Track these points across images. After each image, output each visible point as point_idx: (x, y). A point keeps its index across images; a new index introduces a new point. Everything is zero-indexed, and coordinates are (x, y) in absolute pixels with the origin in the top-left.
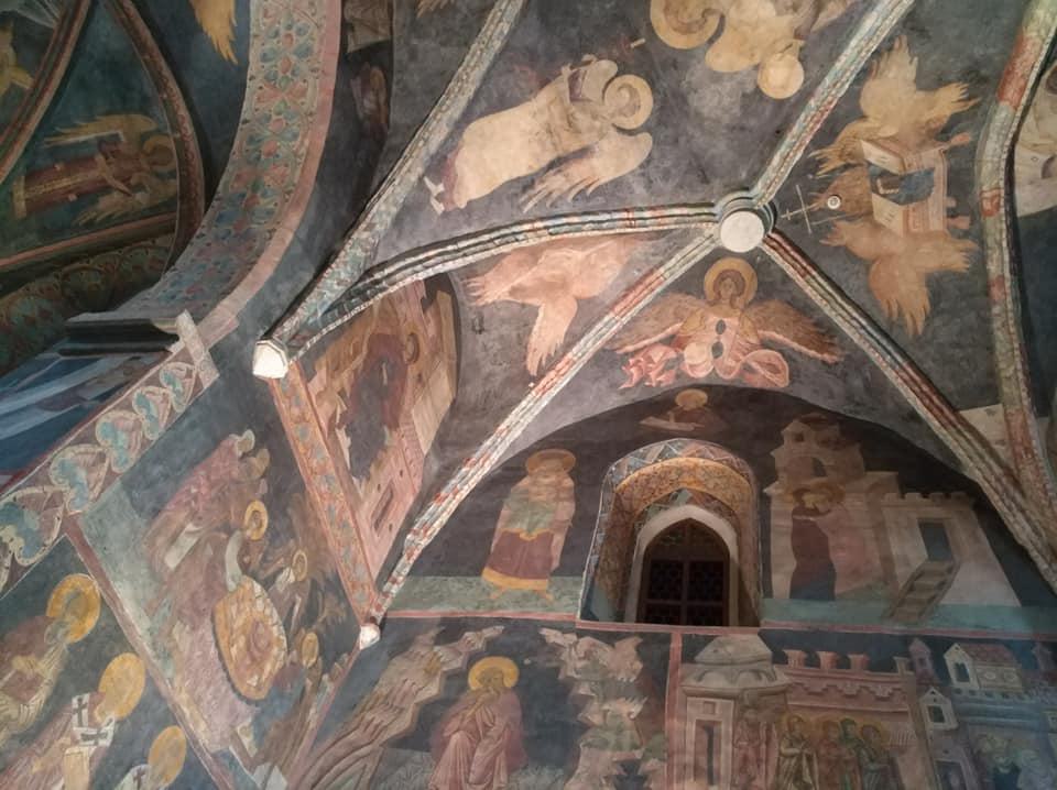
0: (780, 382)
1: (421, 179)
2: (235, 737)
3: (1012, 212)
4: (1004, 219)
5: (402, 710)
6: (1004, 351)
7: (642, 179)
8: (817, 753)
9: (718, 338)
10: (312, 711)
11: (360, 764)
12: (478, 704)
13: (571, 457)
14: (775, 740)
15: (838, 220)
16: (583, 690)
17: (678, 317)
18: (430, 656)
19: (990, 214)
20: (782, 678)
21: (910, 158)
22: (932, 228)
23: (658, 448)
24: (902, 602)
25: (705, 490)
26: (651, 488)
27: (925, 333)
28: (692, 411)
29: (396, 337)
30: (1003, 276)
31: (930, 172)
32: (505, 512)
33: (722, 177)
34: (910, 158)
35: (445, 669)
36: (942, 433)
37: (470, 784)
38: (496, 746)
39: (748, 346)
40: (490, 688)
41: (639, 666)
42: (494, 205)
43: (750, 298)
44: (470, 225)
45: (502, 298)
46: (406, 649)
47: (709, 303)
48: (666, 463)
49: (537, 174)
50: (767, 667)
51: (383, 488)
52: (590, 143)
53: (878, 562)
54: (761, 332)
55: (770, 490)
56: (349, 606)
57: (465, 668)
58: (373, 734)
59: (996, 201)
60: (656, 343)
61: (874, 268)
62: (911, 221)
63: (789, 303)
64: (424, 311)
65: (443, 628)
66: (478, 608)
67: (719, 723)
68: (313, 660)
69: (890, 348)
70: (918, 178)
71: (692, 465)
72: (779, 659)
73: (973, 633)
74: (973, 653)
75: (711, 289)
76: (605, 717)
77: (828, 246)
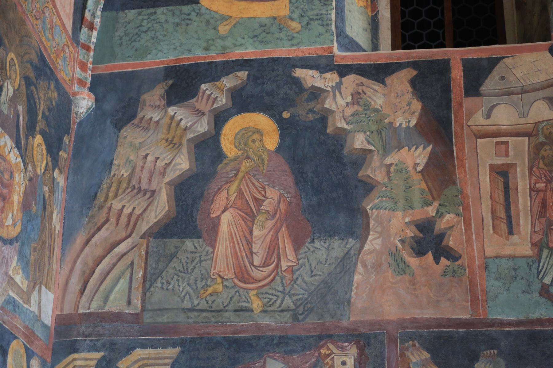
2: (11, 281)
5: (153, 192)
10: (54, 216)
11: (126, 261)
12: (241, 175)
18: (166, 121)
35: (190, 136)
37: (256, 267)
38: (273, 221)
40: (251, 153)
41: (417, 106)
46: (134, 116)
57: (213, 132)
58: (128, 224)
65: (171, 82)
66: (207, 49)
67: (512, 166)
68: (44, 164)
76: (388, 172)
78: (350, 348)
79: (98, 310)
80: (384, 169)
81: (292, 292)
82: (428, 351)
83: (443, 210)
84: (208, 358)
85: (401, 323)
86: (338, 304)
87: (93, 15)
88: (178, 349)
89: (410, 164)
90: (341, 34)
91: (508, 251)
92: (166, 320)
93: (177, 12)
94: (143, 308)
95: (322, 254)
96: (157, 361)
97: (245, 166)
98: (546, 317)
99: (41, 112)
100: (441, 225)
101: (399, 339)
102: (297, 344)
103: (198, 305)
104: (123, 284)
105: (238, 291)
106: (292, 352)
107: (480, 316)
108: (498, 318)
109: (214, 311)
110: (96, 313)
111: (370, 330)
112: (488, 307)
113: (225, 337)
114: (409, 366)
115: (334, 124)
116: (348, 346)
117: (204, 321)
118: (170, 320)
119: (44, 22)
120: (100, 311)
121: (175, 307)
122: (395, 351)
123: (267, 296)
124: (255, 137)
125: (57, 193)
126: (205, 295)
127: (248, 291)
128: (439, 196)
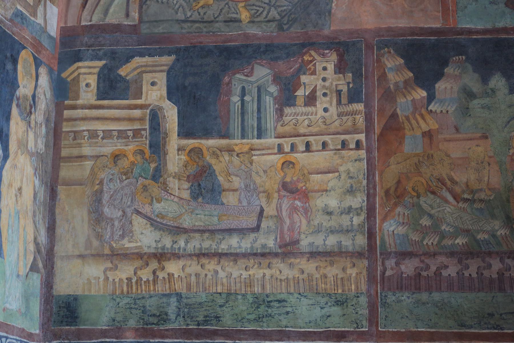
78: (331, 55)
79: (99, 22)
81: (277, 4)
82: (402, 57)
84: (201, 65)
85: (378, 32)
86: (320, 15)
88: (173, 57)
92: (161, 31)
94: (141, 20)
96: (154, 69)
98: (510, 25)
101: (375, 46)
102: (282, 52)
103: (191, 16)
105: (227, 4)
106: (277, 59)
107: (450, 25)
108: (467, 27)
109: (206, 22)
110: (97, 24)
111: (349, 39)
112: (458, 17)
113: (216, 46)
114: (385, 70)
116: (329, 53)
117: (196, 31)
118: (165, 31)
120: (101, 23)
121: (170, 18)
122: (372, 57)
123: (255, 7)
126: (197, 8)
127: (237, 3)
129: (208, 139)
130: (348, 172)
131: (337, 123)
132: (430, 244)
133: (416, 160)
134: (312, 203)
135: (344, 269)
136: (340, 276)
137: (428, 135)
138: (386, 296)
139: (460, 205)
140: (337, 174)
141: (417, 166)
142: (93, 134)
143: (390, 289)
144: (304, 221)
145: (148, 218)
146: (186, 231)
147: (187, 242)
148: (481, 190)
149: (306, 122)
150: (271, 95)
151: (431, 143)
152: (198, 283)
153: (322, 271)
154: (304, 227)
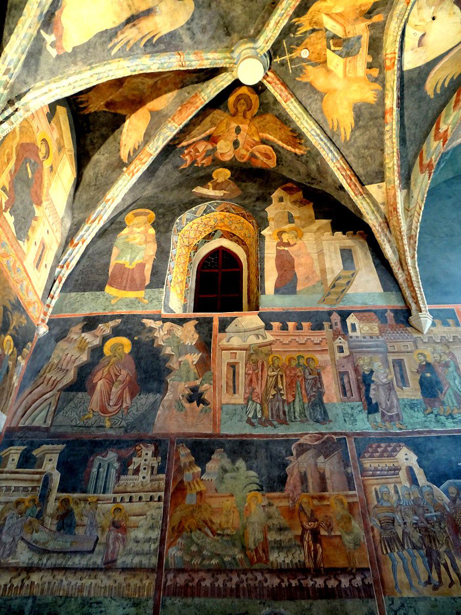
0: (272, 164)
1: (39, 32)
3: (401, 67)
4: (396, 73)
5: (68, 370)
6: (389, 152)
7: (188, 32)
8: (285, 373)
9: (237, 137)
10: (15, 378)
11: (48, 402)
12: (110, 364)
13: (153, 214)
14: (266, 369)
15: (308, 65)
16: (168, 351)
17: (213, 124)
18: (80, 339)
19: (389, 69)
20: (270, 337)
21: (349, 28)
22: (358, 75)
23: (203, 207)
24: (329, 294)
25: (229, 230)
26: (200, 231)
27: (350, 140)
28: (222, 183)
29: (34, 145)
30: (392, 108)
31: (360, 38)
32: (115, 251)
33: (239, 32)
34: (349, 28)
35: (90, 346)
36: (355, 199)
39: (254, 142)
40: (117, 354)
41: (197, 336)
42: (91, 50)
43: (256, 111)
44: (75, 64)
45: (101, 109)
47: (231, 115)
48: (208, 215)
49: (119, 27)
50: (262, 331)
51: (38, 244)
52: (153, 6)
53: (318, 272)
54: (261, 134)
55: (265, 232)
56: (27, 316)
58: (52, 385)
59: (393, 61)
60: (200, 140)
61: (325, 98)
62: (347, 70)
63: (277, 117)
64: (50, 122)
65: (85, 323)
66: (104, 310)
68: (11, 351)
69: (332, 148)
70: (353, 41)
71: (222, 217)
72: (268, 327)
73: (361, 307)
74: (359, 317)
75: (232, 106)
76: (180, 364)
77: (300, 82)
80: (178, 363)
83: (203, 382)
85: (178, 435)
87: (55, 293)
88: (65, 445)
89: (190, 361)
90: (166, 307)
91: (233, 401)
93: (94, 294)
94: (51, 425)
95: (143, 401)
96: (53, 451)
97: (113, 359)
99: (13, 326)
100: (201, 389)
104: (44, 413)
106: (122, 448)
115: (157, 343)
119: (22, 286)
124: (120, 347)
125: (18, 368)
128: (202, 375)
129: (74, 493)
130: (152, 515)
131: (149, 486)
132: (195, 563)
133: (192, 508)
134: (128, 535)
135: (141, 580)
136: (138, 585)
137: (200, 494)
138: (165, 600)
139: (216, 537)
140: (145, 516)
141: (193, 512)
142: (8, 489)
143: (168, 595)
144: (122, 547)
145: (28, 543)
146: (49, 552)
147: (48, 560)
148: (228, 528)
149: (132, 484)
150: (115, 468)
151: (201, 498)
152: (48, 589)
153: (128, 581)
154: (121, 550)
